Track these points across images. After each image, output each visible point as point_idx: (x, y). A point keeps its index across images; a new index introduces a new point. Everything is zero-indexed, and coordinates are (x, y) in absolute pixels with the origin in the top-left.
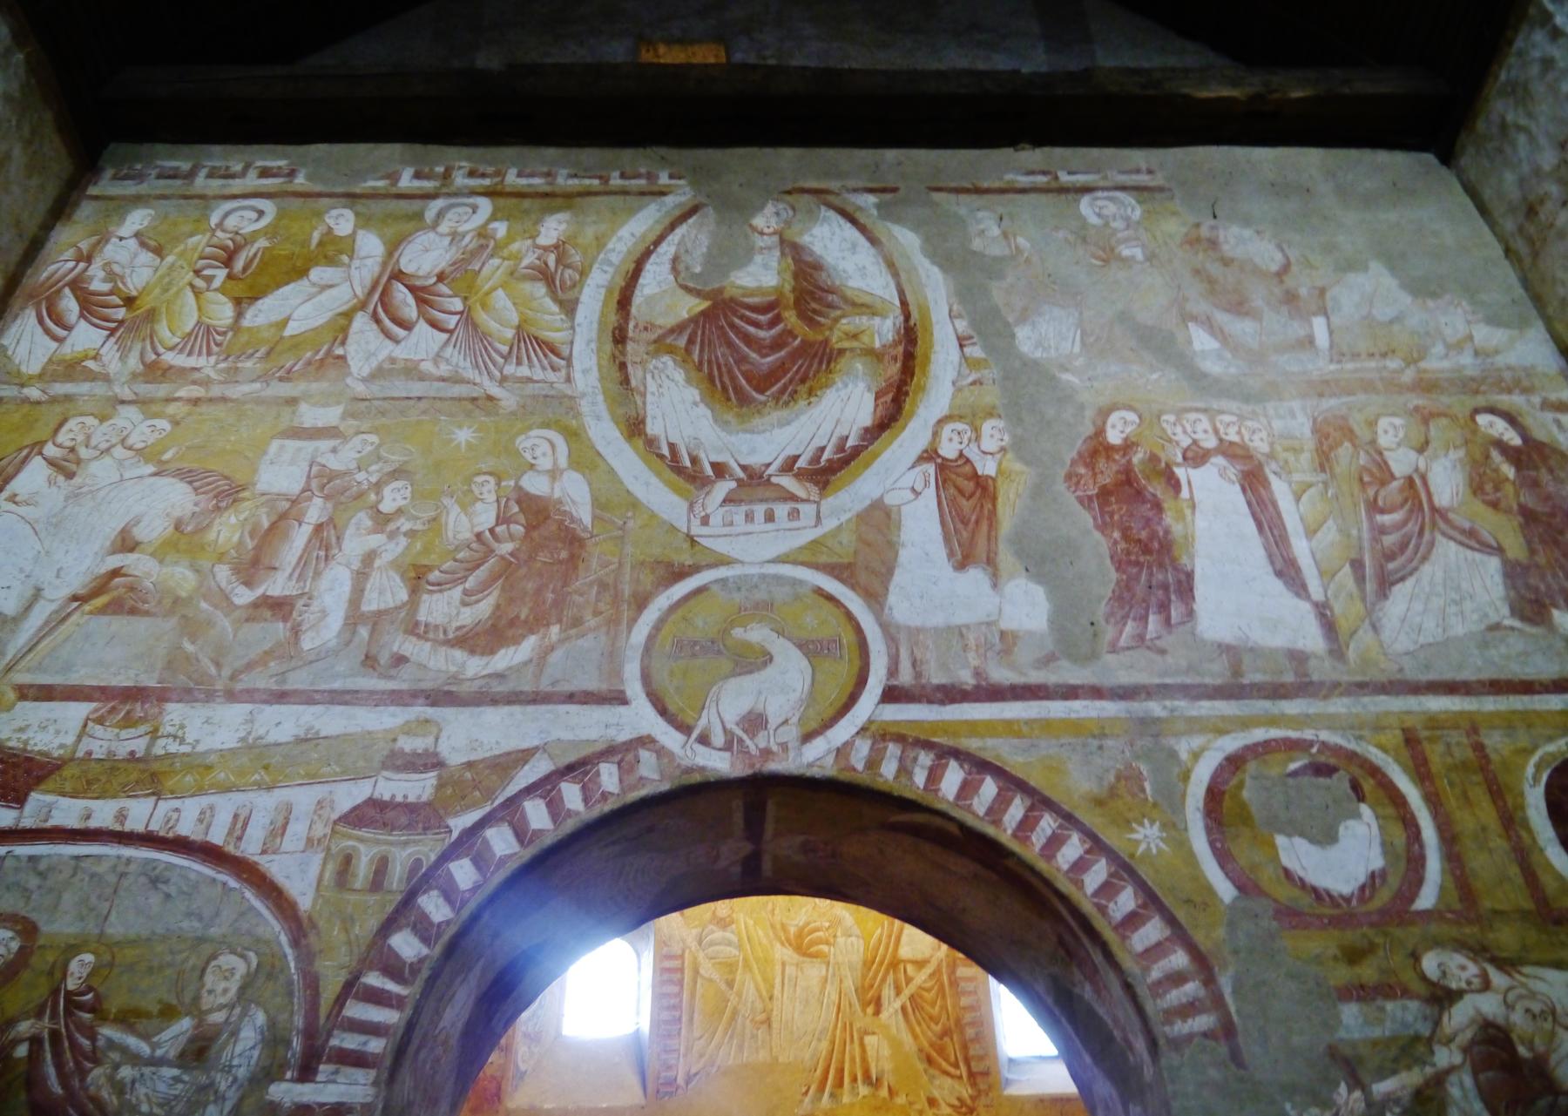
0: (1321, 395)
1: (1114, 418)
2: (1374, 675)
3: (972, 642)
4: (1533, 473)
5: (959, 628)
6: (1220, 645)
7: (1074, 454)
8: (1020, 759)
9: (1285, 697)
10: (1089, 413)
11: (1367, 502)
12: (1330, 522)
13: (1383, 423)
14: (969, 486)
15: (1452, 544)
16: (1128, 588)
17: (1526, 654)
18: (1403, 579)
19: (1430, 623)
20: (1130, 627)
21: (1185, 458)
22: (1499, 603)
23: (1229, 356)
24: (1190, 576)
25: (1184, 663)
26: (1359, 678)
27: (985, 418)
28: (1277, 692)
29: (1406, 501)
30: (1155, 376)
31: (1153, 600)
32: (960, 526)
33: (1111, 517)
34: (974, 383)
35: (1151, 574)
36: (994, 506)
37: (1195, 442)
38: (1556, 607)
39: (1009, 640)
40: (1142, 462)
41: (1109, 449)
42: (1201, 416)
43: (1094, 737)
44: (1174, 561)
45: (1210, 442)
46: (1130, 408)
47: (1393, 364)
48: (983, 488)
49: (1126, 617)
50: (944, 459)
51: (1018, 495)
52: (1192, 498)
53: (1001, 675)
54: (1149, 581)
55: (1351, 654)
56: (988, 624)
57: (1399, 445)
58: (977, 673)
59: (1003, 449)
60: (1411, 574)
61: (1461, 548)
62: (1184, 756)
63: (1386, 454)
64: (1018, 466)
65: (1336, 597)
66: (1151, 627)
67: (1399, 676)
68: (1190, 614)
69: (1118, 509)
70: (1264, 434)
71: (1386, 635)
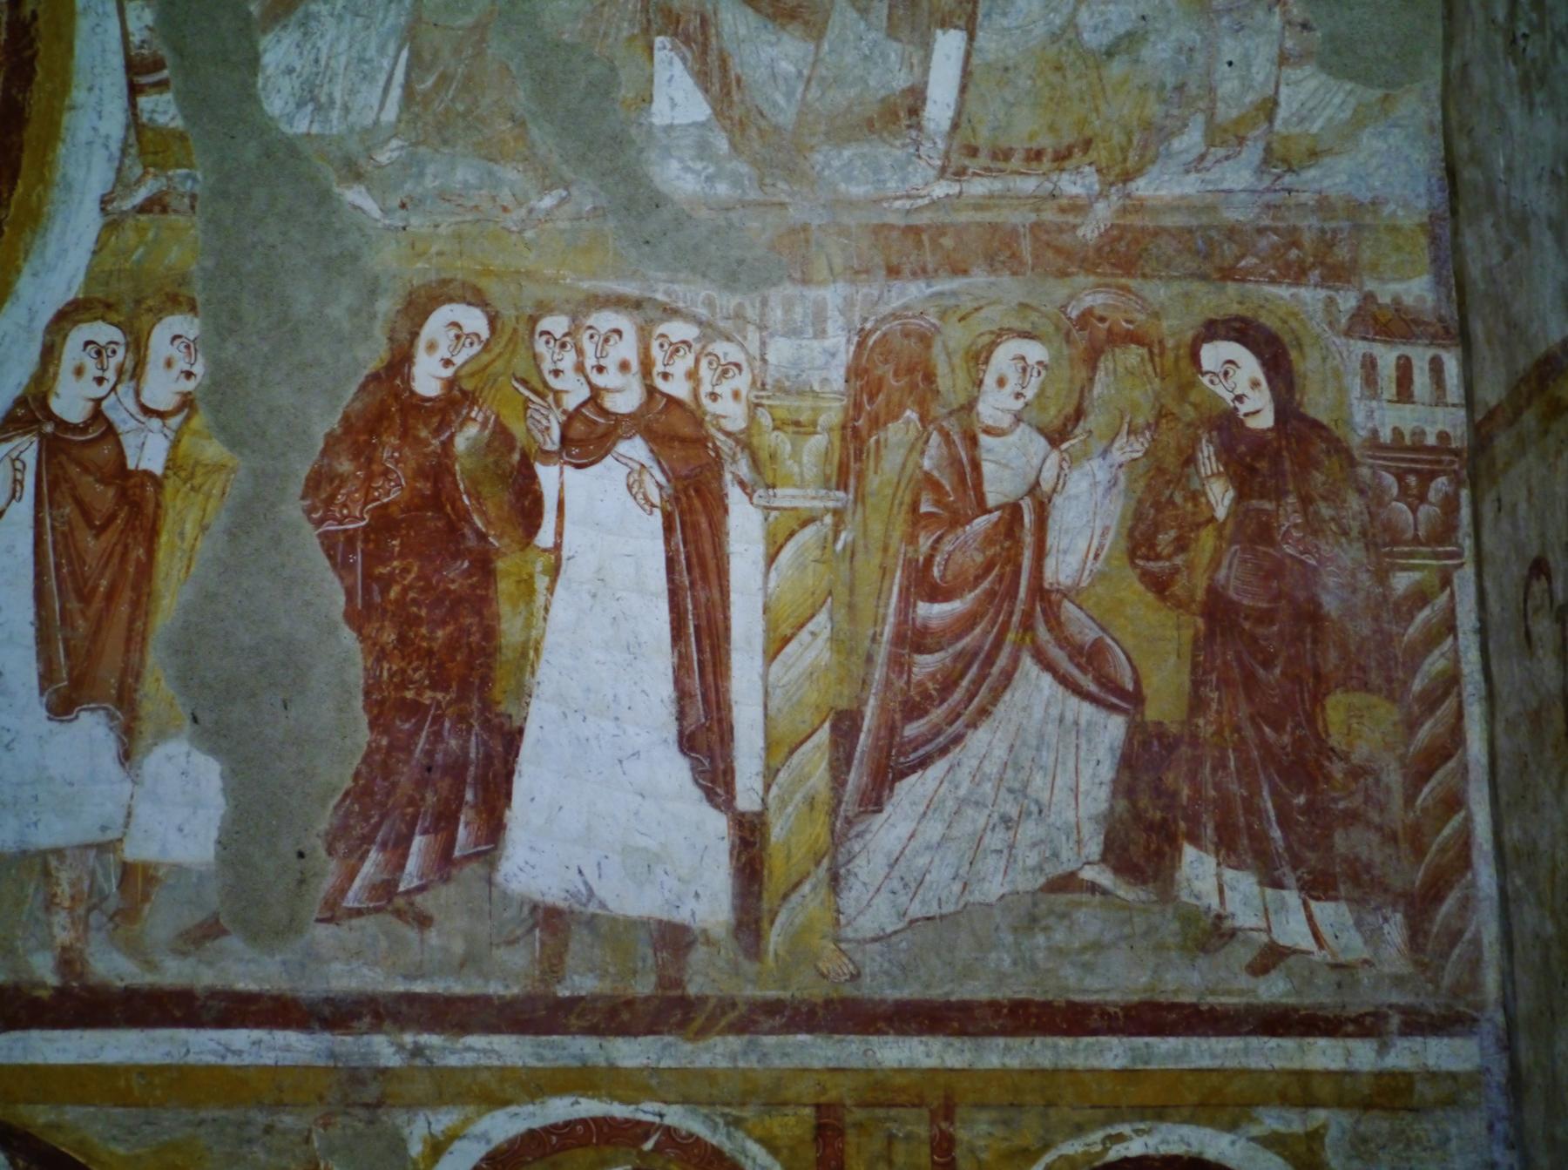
0: (893, 272)
1: (436, 324)
2: (805, 987)
3: (64, 890)
4: (1268, 506)
5: (43, 854)
6: (535, 907)
7: (334, 422)
8: (121, 1150)
9: (625, 1031)
10: (386, 306)
11: (909, 563)
12: (822, 618)
13: (1004, 356)
14: (103, 497)
15: (1047, 679)
16: (387, 771)
17: (1097, 946)
18: (924, 763)
19: (940, 875)
20: (372, 865)
21: (564, 439)
22: (1088, 829)
23: (722, 144)
24: (512, 739)
25: (458, 947)
26: (772, 993)
27: (158, 314)
28: (614, 1017)
29: (988, 567)
30: (548, 202)
31: (431, 798)
32: (74, 605)
33: (384, 591)
34: (142, 209)
35: (437, 736)
36: (151, 552)
37: (596, 394)
38: (1195, 840)
39: (138, 880)
40: (472, 451)
41: (416, 406)
42: (622, 321)
43: (260, 1105)
44: (487, 705)
45: (625, 399)
46: (477, 299)
47: (1073, 185)
48: (137, 503)
49: (368, 839)
50: (61, 424)
51: (204, 528)
52: (558, 547)
53: (112, 966)
54: (430, 754)
55: (775, 939)
56: (102, 848)
57: (1018, 418)
58: (68, 962)
59: (187, 403)
60: (944, 751)
61: (1060, 690)
62: (416, 1149)
63: (984, 440)
64: (213, 450)
65: (783, 804)
66: (412, 864)
67: (848, 991)
68: (494, 829)
69: (403, 571)
70: (742, 382)
71: (850, 899)
